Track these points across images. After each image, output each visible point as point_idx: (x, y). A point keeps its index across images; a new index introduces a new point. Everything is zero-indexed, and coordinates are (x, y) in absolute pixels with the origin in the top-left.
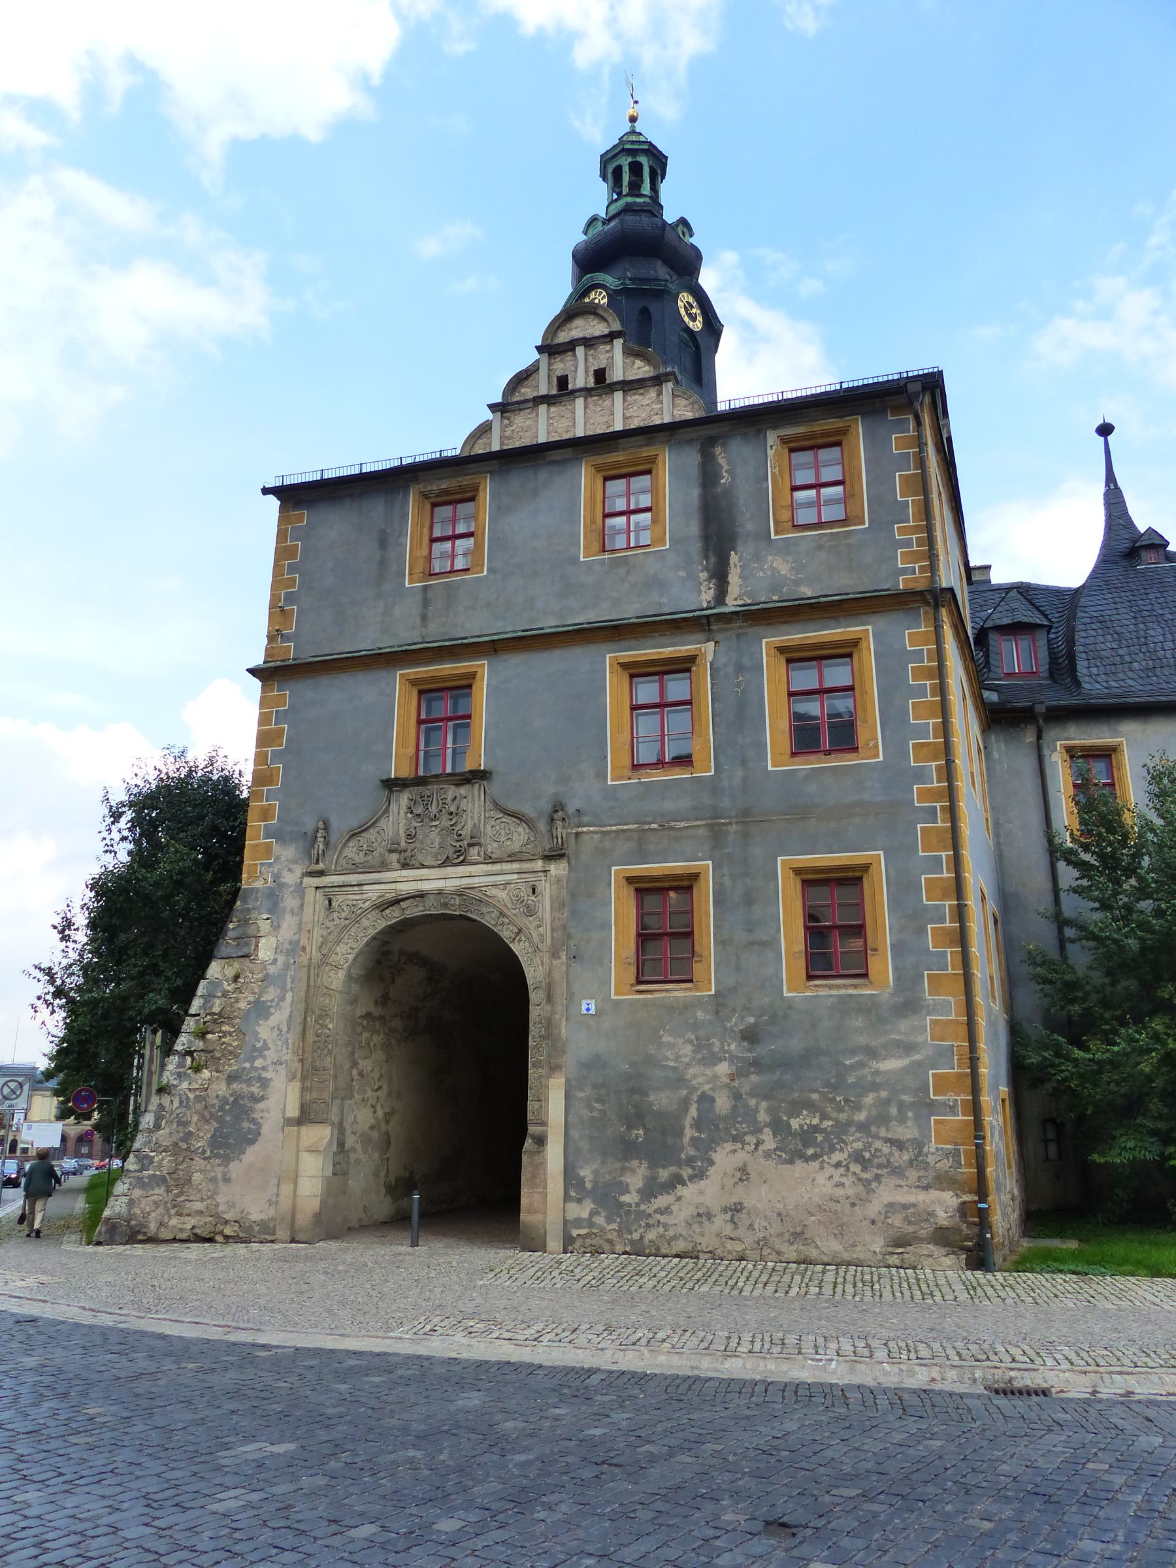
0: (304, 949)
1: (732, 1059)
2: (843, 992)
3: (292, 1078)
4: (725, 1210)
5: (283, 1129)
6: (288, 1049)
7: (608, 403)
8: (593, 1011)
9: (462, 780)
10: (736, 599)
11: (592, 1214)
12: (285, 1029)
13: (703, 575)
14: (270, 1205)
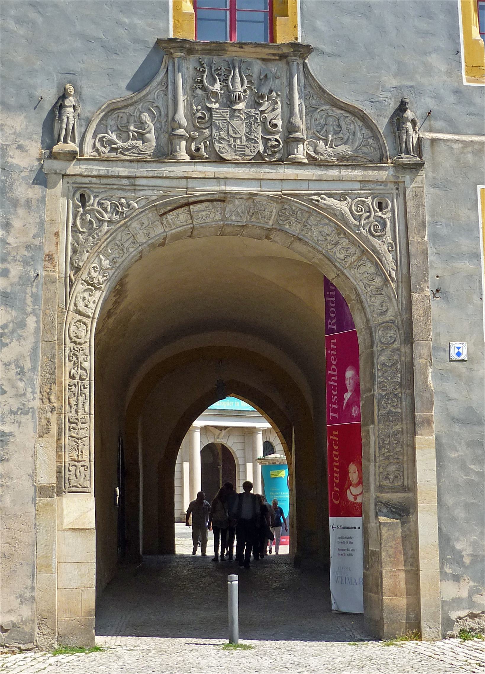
0: (50, 258)
5: (34, 499)
6: (33, 392)
8: (464, 356)
9: (274, 55)
12: (28, 365)
14: (22, 603)
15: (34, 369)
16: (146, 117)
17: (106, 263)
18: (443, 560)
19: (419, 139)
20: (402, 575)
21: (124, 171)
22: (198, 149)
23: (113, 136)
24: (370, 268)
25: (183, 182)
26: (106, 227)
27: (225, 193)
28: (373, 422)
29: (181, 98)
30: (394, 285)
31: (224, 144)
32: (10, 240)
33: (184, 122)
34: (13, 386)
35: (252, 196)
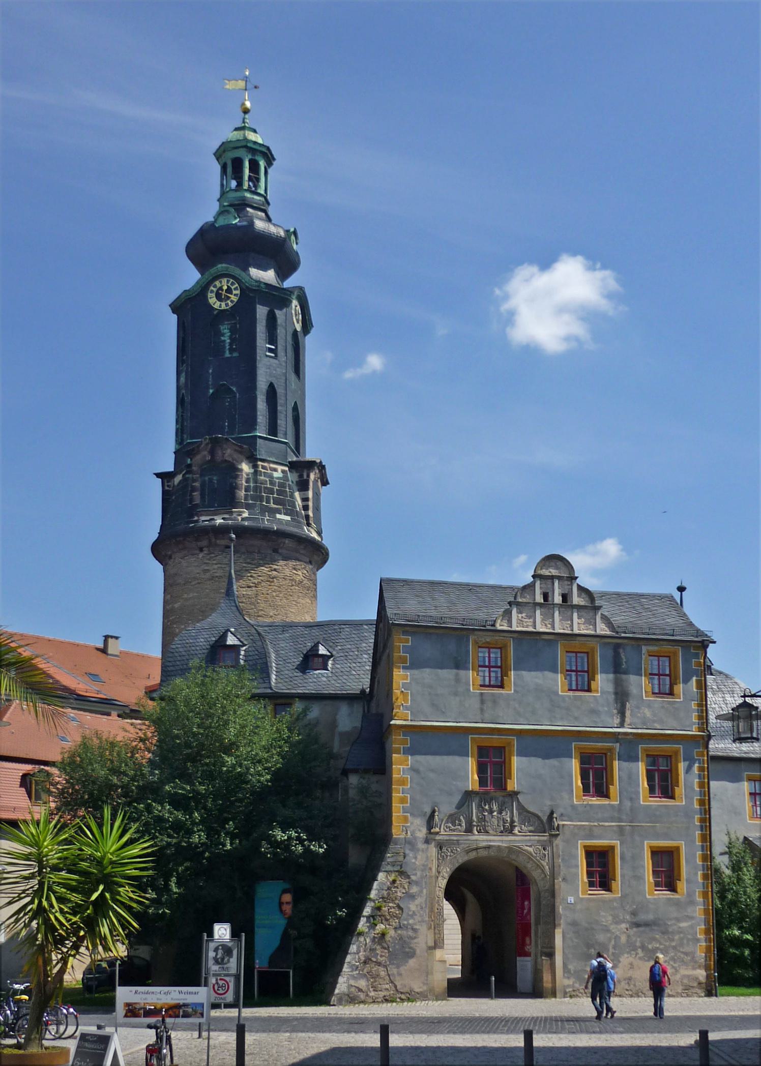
0: (430, 869)
1: (628, 922)
2: (668, 896)
3: (430, 928)
4: (625, 980)
5: (427, 951)
7: (569, 613)
8: (573, 902)
10: (628, 725)
11: (573, 983)
12: (424, 906)
13: (615, 711)
15: (426, 907)
16: (462, 818)
17: (448, 870)
18: (564, 972)
19: (558, 824)
20: (550, 977)
21: (455, 838)
22: (480, 830)
23: (451, 825)
24: (540, 871)
25: (475, 842)
26: (449, 857)
27: (490, 845)
28: (540, 924)
29: (474, 811)
30: (548, 877)
31: (489, 828)
32: (417, 863)
33: (475, 820)
34: (419, 913)
35: (499, 846)
